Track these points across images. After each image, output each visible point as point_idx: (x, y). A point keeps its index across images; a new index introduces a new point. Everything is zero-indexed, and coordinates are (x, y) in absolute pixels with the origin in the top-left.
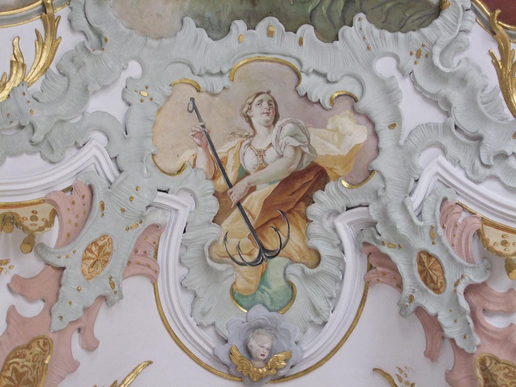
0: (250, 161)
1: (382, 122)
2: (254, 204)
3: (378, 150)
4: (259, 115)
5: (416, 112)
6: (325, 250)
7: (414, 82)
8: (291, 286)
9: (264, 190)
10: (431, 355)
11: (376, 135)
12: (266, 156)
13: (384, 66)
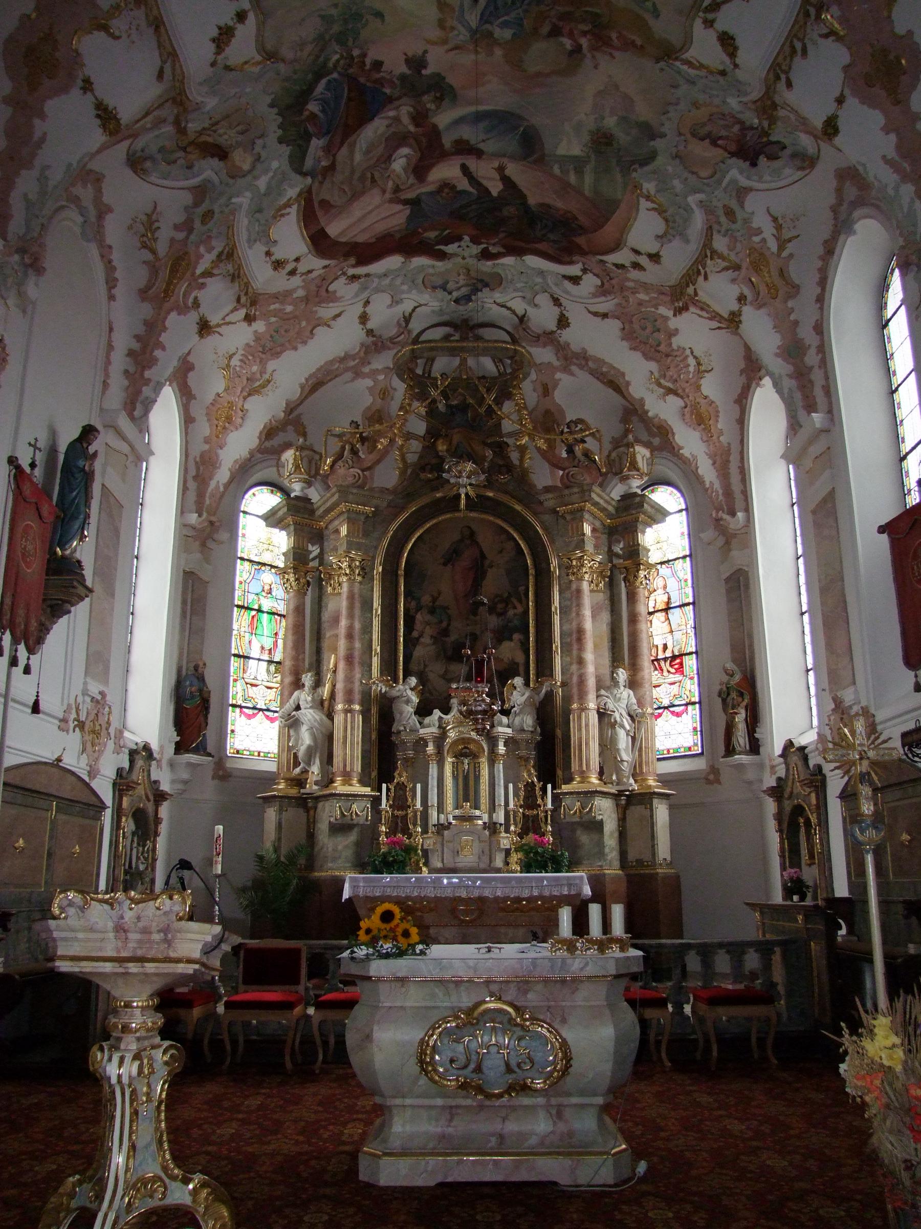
0: (221, 131)
1: (255, 173)
2: (204, 138)
3: (244, 176)
4: (239, 128)
5: (262, 183)
6: (196, 169)
7: (273, 177)
8: (175, 162)
9: (210, 140)
10: (176, 227)
11: (250, 171)
12: (226, 136)
13: (275, 164)
